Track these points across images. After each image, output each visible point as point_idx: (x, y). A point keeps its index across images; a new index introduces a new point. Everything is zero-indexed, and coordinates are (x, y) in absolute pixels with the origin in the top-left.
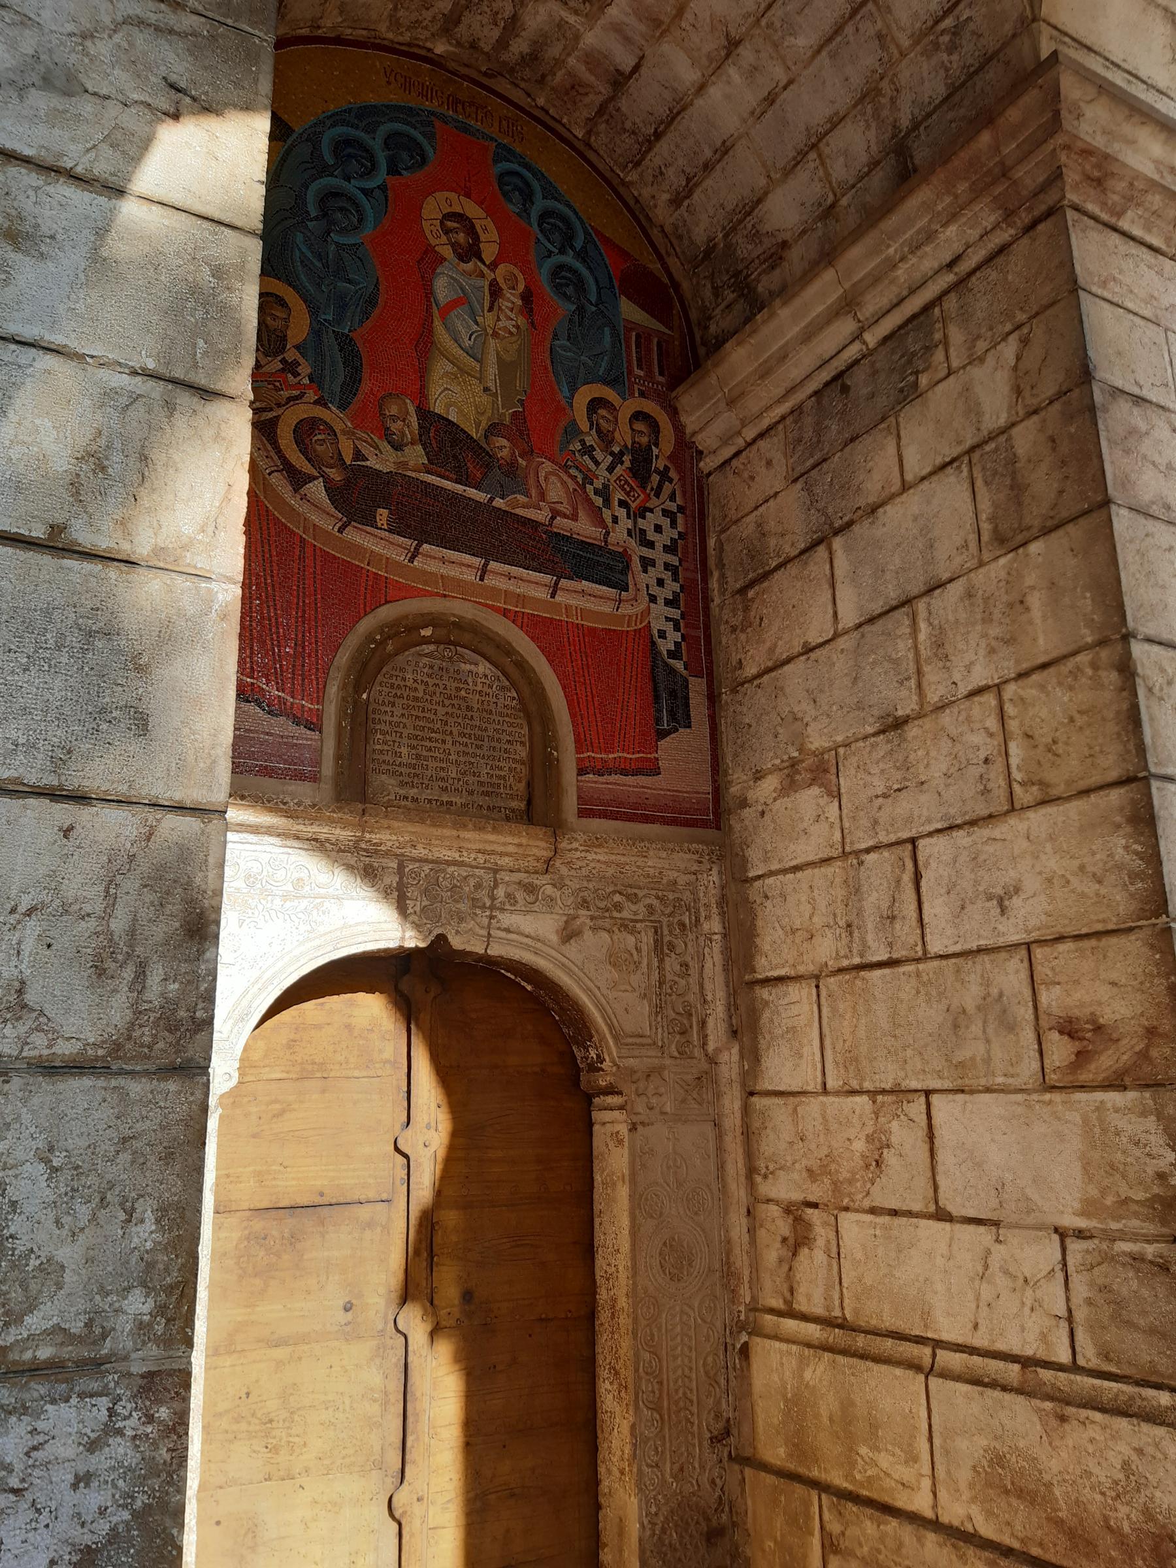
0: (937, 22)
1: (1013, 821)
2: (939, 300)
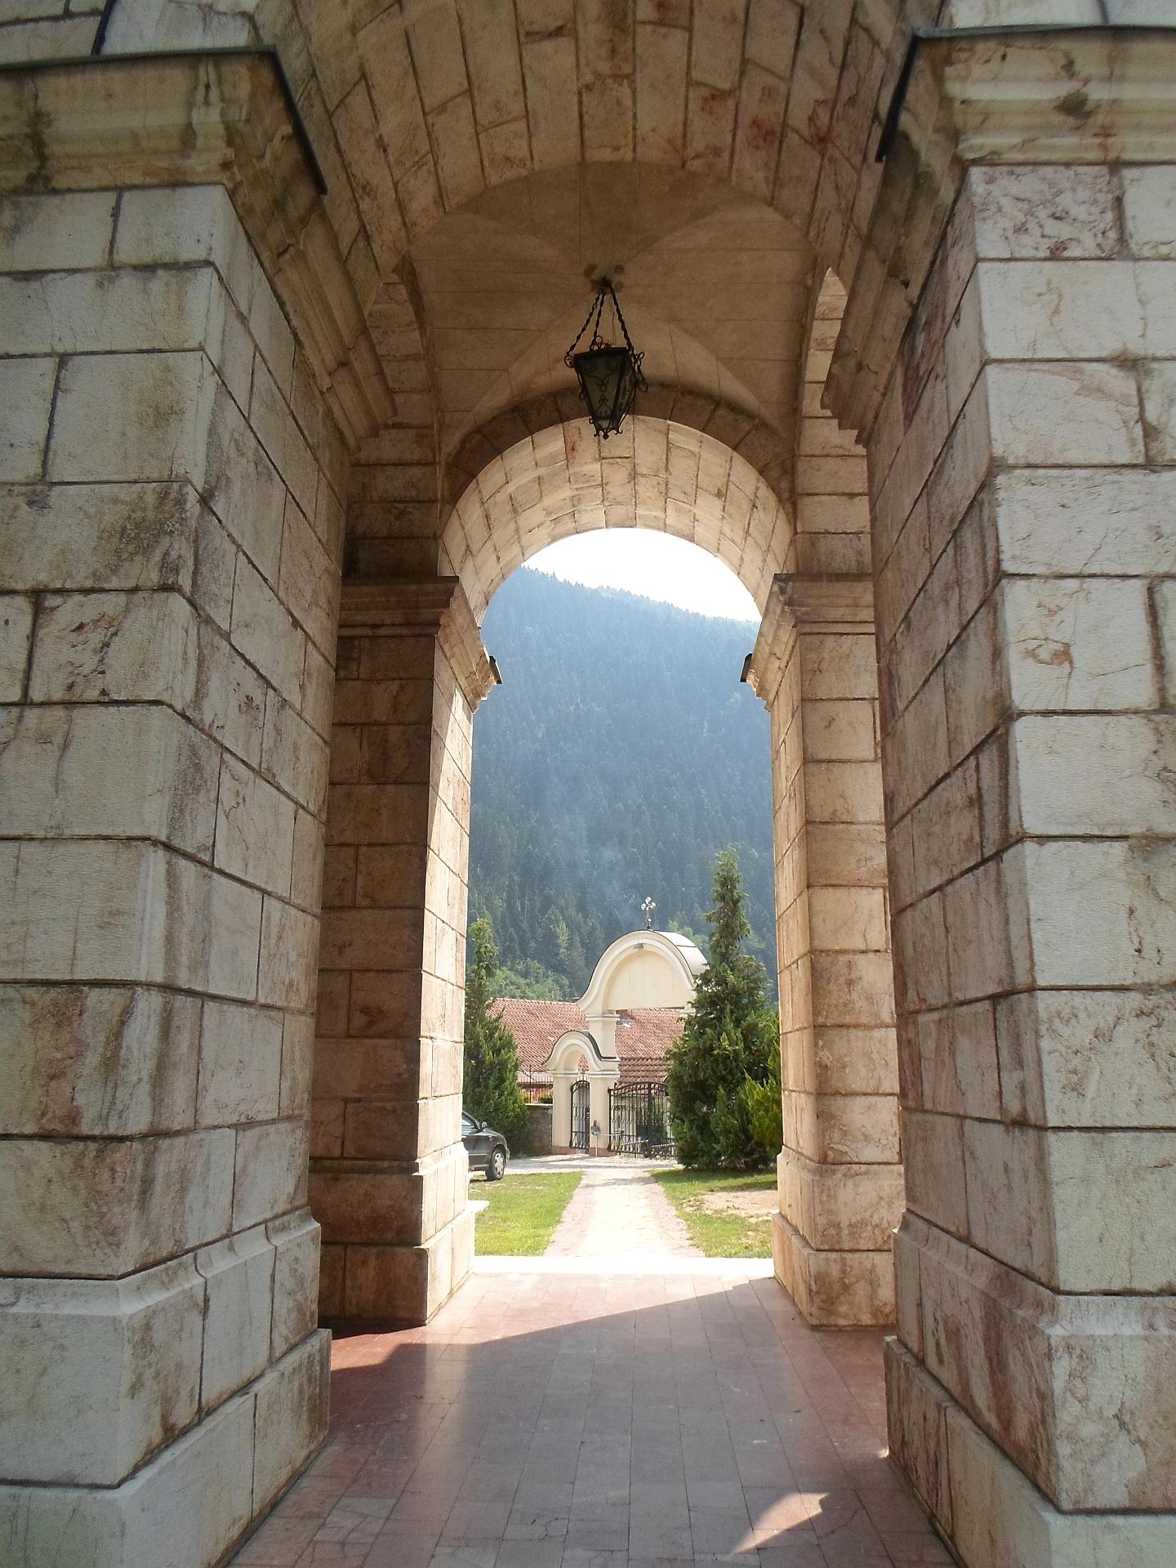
0: (395, 501)
1: (353, 912)
2: (360, 637)
